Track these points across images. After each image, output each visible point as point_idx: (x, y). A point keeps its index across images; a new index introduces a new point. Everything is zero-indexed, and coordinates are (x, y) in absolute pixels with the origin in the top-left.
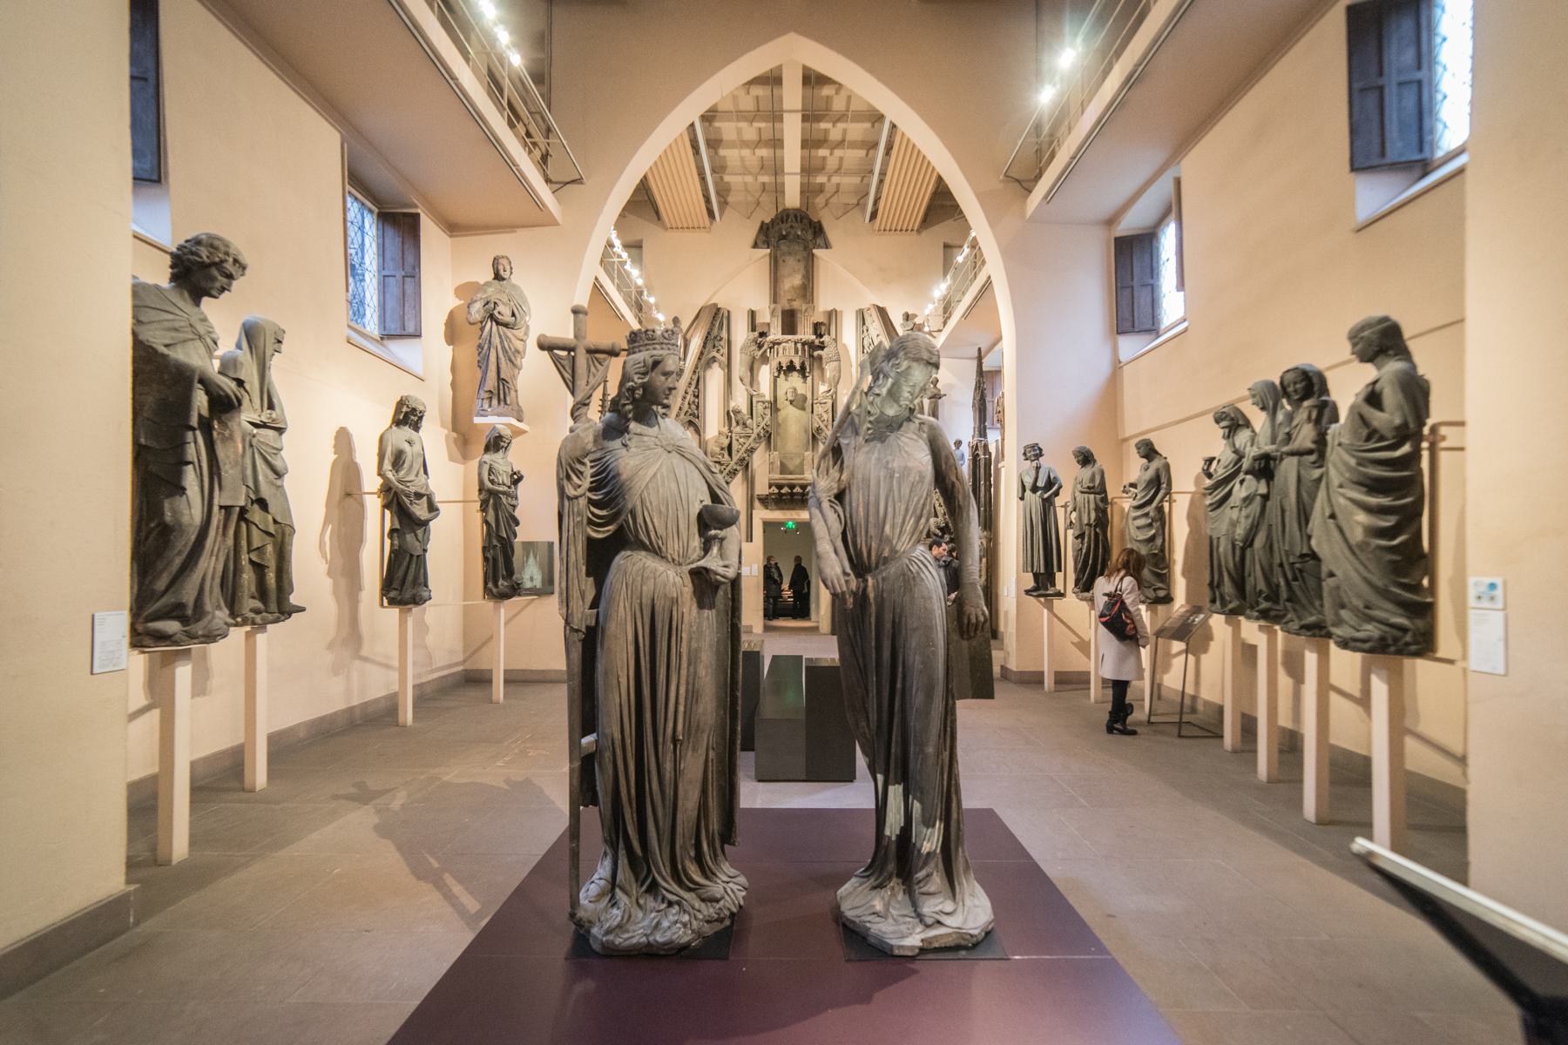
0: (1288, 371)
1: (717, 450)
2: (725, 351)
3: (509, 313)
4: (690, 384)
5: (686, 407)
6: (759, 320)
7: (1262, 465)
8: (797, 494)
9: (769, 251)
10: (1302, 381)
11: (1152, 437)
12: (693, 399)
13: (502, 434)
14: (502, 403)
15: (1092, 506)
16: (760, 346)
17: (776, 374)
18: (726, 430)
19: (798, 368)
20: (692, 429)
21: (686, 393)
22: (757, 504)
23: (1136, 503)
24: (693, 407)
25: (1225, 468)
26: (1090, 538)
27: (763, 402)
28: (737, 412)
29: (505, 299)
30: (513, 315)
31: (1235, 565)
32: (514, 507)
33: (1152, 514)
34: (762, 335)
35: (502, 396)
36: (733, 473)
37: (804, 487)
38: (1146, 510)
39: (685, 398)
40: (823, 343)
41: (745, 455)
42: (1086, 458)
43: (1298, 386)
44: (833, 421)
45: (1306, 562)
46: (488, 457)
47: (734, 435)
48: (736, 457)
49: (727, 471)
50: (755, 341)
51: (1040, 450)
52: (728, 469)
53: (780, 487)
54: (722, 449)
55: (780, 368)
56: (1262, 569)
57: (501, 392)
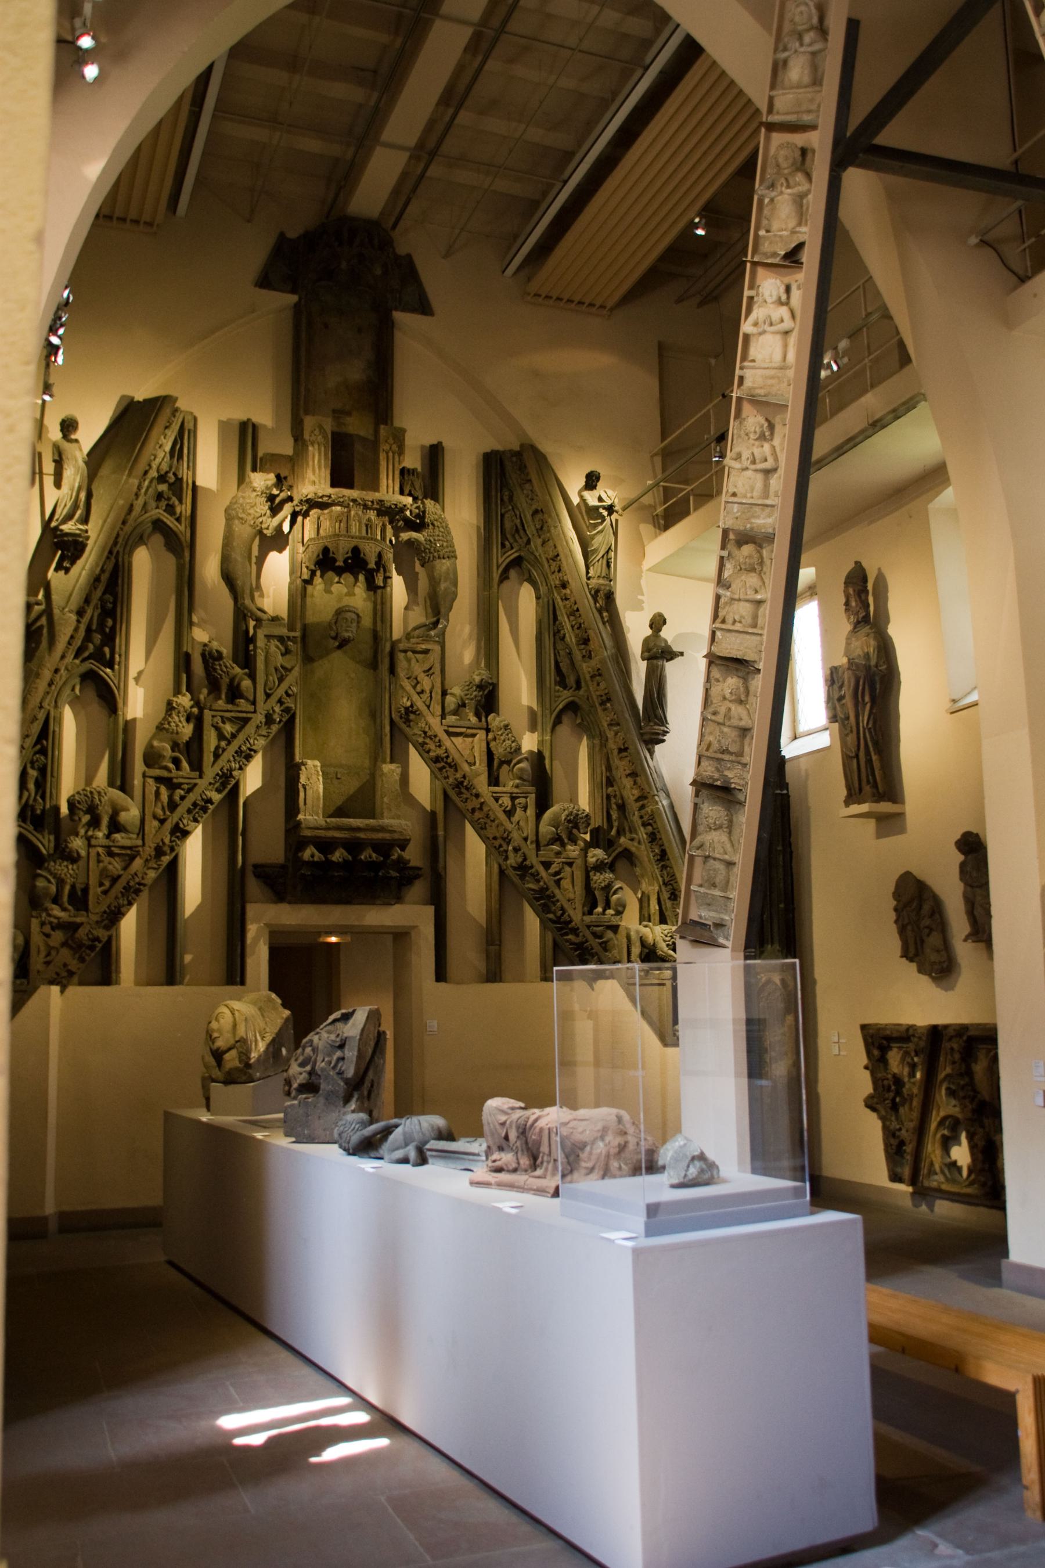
18: (185, 701)
22: (253, 886)
24: (97, 638)
27: (281, 639)
28: (210, 658)
37: (384, 848)
40: (421, 515)
44: (444, 693)
47: (207, 714)
48: (210, 772)
49: (187, 803)
53: (325, 846)
54: (175, 746)
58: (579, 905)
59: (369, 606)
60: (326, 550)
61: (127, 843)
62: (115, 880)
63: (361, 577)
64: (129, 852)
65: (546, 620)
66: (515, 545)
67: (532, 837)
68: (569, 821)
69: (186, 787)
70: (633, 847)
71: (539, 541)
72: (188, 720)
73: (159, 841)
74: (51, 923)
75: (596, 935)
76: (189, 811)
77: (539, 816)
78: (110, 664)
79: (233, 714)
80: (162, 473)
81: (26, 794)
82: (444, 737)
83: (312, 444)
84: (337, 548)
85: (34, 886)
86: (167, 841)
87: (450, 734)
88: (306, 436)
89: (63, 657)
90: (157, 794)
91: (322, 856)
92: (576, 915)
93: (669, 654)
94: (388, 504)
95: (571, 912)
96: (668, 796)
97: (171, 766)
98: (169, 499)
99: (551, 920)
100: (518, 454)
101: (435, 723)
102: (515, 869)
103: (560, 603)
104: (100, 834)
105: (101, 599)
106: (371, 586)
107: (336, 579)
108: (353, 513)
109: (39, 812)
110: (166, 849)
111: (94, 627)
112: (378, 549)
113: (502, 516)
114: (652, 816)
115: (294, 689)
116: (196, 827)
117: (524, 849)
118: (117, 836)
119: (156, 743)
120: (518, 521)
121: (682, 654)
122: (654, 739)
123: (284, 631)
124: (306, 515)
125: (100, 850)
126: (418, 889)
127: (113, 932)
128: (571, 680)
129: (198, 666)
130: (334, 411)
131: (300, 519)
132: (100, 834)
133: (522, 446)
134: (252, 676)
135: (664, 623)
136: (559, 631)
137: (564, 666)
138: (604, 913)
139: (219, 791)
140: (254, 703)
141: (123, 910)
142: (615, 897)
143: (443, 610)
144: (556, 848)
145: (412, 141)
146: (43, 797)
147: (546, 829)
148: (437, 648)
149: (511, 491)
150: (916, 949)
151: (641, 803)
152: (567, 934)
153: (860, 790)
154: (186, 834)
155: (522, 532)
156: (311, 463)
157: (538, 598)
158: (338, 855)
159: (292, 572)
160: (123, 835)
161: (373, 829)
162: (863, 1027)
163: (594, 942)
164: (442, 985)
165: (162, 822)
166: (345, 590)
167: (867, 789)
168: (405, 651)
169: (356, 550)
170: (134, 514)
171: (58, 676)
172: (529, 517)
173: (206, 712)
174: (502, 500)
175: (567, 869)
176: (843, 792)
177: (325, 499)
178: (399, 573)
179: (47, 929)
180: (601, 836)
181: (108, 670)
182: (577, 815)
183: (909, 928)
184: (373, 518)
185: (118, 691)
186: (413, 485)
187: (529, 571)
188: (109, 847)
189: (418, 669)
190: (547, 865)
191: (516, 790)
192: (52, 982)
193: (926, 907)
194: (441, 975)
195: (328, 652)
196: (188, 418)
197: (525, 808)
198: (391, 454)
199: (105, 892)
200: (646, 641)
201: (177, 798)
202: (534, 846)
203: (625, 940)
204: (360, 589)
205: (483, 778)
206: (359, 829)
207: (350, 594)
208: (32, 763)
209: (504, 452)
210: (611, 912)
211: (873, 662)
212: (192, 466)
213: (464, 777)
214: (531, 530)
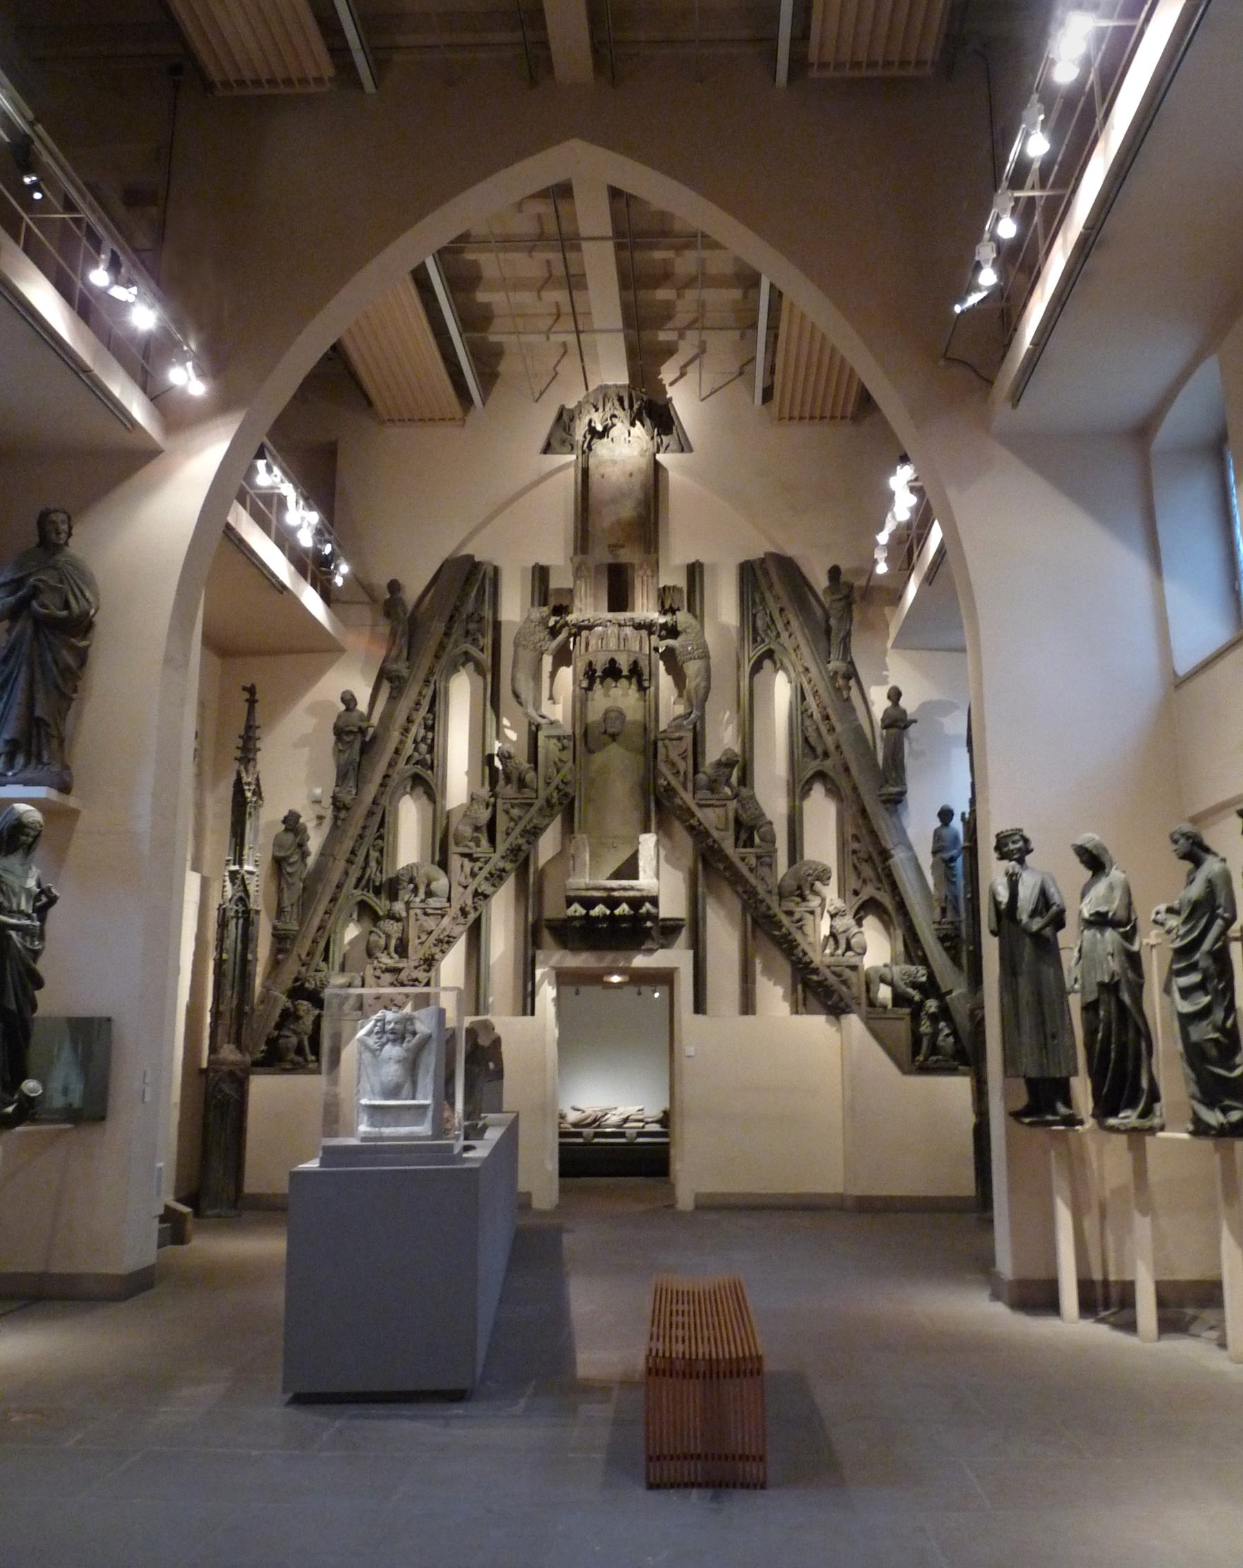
1: (467, 831)
2: (487, 641)
4: (418, 704)
5: (409, 748)
6: (555, 583)
8: (623, 918)
12: (422, 732)
13: (25, 819)
14: (34, 761)
16: (554, 632)
17: (585, 684)
18: (485, 792)
19: (625, 672)
20: (420, 790)
21: (410, 720)
22: (547, 936)
24: (423, 747)
26: (1108, 1012)
27: (559, 738)
32: (36, 954)
33: (1202, 964)
34: (560, 610)
35: (34, 749)
36: (497, 878)
37: (636, 903)
39: (406, 731)
41: (521, 841)
42: (1094, 862)
48: (502, 847)
49: (484, 873)
50: (544, 622)
51: (1026, 841)
52: (487, 868)
54: (477, 829)
55: (590, 673)
57: (34, 741)
60: (590, 663)
61: (438, 906)
62: (430, 933)
64: (439, 912)
65: (794, 704)
66: (767, 640)
67: (776, 891)
69: (482, 860)
72: (487, 807)
73: (461, 902)
74: (380, 968)
75: (834, 973)
76: (486, 878)
78: (432, 767)
79: (519, 801)
81: (368, 871)
82: (695, 808)
85: (369, 941)
86: (469, 902)
87: (701, 806)
90: (462, 866)
91: (584, 912)
97: (472, 844)
98: (474, 634)
101: (687, 797)
103: (806, 685)
104: (418, 900)
105: (424, 718)
106: (642, 689)
107: (614, 684)
108: (609, 632)
109: (377, 884)
110: (467, 909)
111: (419, 739)
115: (569, 778)
116: (494, 892)
117: (768, 900)
118: (430, 900)
119: (461, 827)
120: (768, 619)
125: (418, 911)
126: (683, 937)
127: (432, 974)
128: (819, 751)
129: (497, 763)
131: (578, 638)
132: (418, 900)
134: (536, 769)
136: (806, 710)
137: (813, 740)
138: (843, 955)
139: (511, 861)
140: (537, 791)
141: (437, 957)
146: (381, 872)
149: (762, 593)
154: (486, 897)
155: (772, 627)
157: (790, 682)
159: (574, 683)
160: (435, 899)
161: (624, 889)
164: (700, 1017)
165: (465, 887)
168: (663, 740)
169: (613, 662)
173: (499, 800)
174: (754, 602)
177: (586, 623)
179: (378, 973)
181: (429, 772)
182: (816, 869)
184: (629, 633)
185: (436, 785)
186: (673, 599)
187: (781, 661)
188: (424, 909)
189: (674, 755)
194: (699, 1006)
195: (605, 745)
198: (645, 578)
199: (422, 943)
201: (476, 869)
202: (776, 898)
204: (633, 692)
205: (731, 841)
206: (613, 890)
208: (374, 846)
209: (754, 561)
213: (714, 841)
214: (780, 626)
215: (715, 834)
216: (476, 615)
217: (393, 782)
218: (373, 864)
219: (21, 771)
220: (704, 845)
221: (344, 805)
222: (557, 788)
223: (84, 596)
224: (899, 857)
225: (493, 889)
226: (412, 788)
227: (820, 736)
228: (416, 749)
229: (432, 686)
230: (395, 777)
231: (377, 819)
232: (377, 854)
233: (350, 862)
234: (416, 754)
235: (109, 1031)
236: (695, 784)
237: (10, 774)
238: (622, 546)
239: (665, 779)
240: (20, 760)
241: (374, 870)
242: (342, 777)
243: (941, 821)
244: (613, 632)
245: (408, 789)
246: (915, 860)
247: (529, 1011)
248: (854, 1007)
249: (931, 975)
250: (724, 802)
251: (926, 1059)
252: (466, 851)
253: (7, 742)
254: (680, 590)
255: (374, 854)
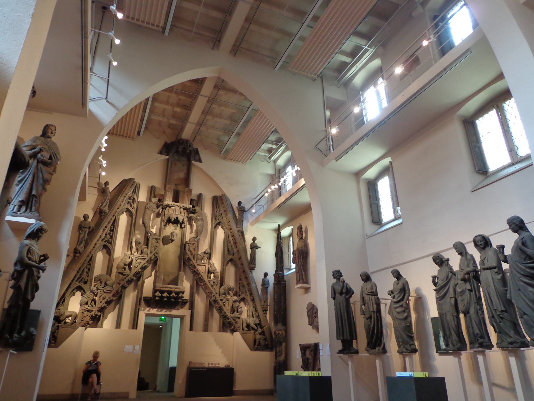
0: (477, 236)
3: (48, 157)
4: (109, 222)
7: (474, 274)
9: (168, 157)
10: (483, 240)
11: (398, 268)
12: (109, 231)
14: (28, 210)
15: (374, 302)
20: (105, 250)
21: (106, 227)
23: (395, 300)
24: (108, 236)
25: (442, 281)
26: (374, 318)
27: (156, 239)
29: (47, 148)
30: (50, 158)
31: (455, 326)
35: (30, 205)
36: (129, 282)
37: (177, 293)
38: (401, 303)
39: (104, 230)
40: (195, 210)
43: (482, 242)
45: (504, 314)
46: (27, 242)
52: (127, 278)
53: (162, 292)
56: (476, 323)
58: (230, 312)
59: (181, 232)
63: (179, 225)
67: (218, 293)
68: (228, 289)
70: (245, 297)
71: (225, 218)
75: (234, 320)
76: (127, 282)
77: (220, 288)
78: (111, 243)
80: (130, 197)
81: (83, 276)
83: (168, 192)
84: (172, 217)
88: (167, 190)
89: (98, 241)
91: (161, 295)
92: (229, 314)
93: (257, 247)
94: (186, 207)
95: (227, 313)
96: (255, 284)
97: (123, 270)
99: (222, 315)
100: (221, 197)
102: (213, 301)
103: (229, 234)
104: (101, 286)
105: (110, 227)
106: (181, 227)
111: (107, 234)
112: (183, 218)
113: (216, 211)
114: (251, 289)
118: (106, 287)
121: (260, 247)
122: (252, 269)
123: (157, 237)
124: (165, 209)
125: (101, 291)
126: (188, 305)
130: (175, 184)
131: (164, 210)
133: (222, 195)
135: (256, 239)
136: (229, 241)
140: (147, 255)
142: (239, 310)
143: (199, 234)
144: (224, 296)
145: (196, 122)
146: (88, 276)
147: (222, 290)
148: (196, 243)
149: (219, 205)
150: (312, 323)
151: (248, 285)
152: (226, 319)
153: (299, 281)
156: (167, 196)
157: (224, 232)
158: (165, 294)
160: (108, 287)
162: (300, 345)
163: (233, 322)
165: (119, 284)
166: (174, 228)
167: (301, 280)
169: (177, 218)
170: (121, 206)
171: (96, 245)
172: (223, 212)
175: (227, 302)
176: (296, 282)
178: (189, 225)
179: (83, 311)
180: (237, 293)
181: (110, 245)
182: (230, 287)
183: (310, 316)
185: (112, 250)
188: (104, 290)
189: (191, 249)
190: (221, 300)
191: (214, 280)
192: (83, 326)
193: (314, 311)
194: (191, 329)
196: (138, 184)
197: (217, 285)
199: (101, 302)
200: (251, 244)
202: (218, 295)
203: (241, 321)
206: (171, 288)
207: (176, 229)
208: (86, 267)
210: (238, 314)
211: (303, 249)
212: (138, 196)
213: (201, 276)
214: (223, 215)
215: (202, 274)
216: (132, 197)
217: (97, 246)
218: (85, 273)
219: (23, 212)
220: (198, 277)
221: (79, 252)
222: (154, 254)
223: (57, 157)
224: (253, 285)
225: (128, 285)
226: (102, 249)
227: (232, 248)
228: (105, 237)
229: (115, 217)
230: (98, 245)
231: (89, 258)
232: (87, 270)
233: (78, 272)
234: (106, 238)
235: (38, 316)
236: (197, 258)
237: (19, 213)
238: (179, 185)
239: (188, 256)
240: (23, 209)
241: (85, 275)
242: (79, 242)
243: (264, 276)
244: (178, 209)
245: (101, 250)
246: (256, 287)
247: (135, 328)
248: (239, 330)
249: (260, 321)
250: (205, 265)
251: (257, 347)
252: (122, 272)
253: (20, 201)
254: (195, 201)
255: (86, 270)
